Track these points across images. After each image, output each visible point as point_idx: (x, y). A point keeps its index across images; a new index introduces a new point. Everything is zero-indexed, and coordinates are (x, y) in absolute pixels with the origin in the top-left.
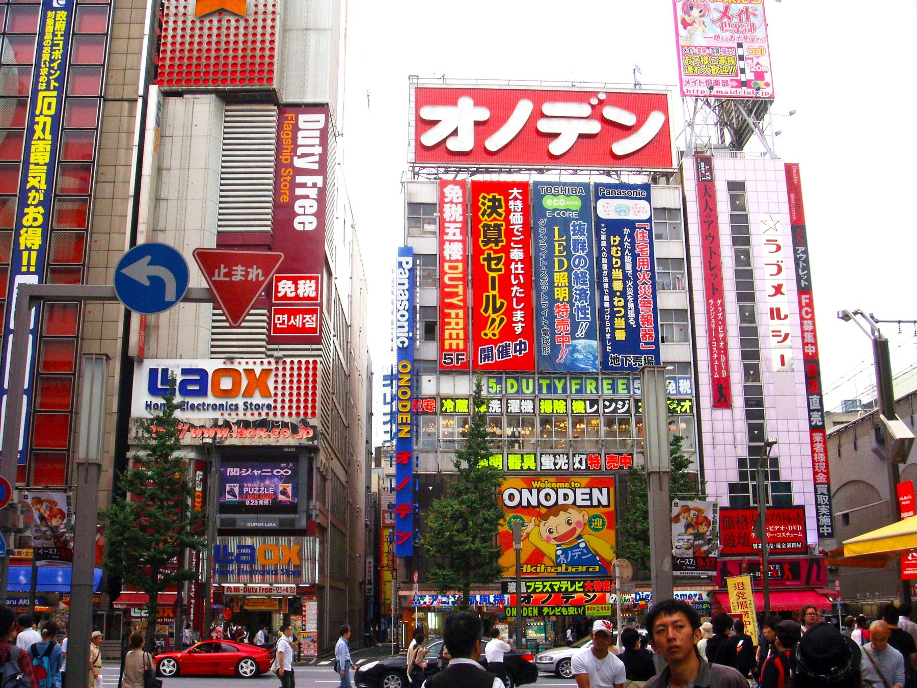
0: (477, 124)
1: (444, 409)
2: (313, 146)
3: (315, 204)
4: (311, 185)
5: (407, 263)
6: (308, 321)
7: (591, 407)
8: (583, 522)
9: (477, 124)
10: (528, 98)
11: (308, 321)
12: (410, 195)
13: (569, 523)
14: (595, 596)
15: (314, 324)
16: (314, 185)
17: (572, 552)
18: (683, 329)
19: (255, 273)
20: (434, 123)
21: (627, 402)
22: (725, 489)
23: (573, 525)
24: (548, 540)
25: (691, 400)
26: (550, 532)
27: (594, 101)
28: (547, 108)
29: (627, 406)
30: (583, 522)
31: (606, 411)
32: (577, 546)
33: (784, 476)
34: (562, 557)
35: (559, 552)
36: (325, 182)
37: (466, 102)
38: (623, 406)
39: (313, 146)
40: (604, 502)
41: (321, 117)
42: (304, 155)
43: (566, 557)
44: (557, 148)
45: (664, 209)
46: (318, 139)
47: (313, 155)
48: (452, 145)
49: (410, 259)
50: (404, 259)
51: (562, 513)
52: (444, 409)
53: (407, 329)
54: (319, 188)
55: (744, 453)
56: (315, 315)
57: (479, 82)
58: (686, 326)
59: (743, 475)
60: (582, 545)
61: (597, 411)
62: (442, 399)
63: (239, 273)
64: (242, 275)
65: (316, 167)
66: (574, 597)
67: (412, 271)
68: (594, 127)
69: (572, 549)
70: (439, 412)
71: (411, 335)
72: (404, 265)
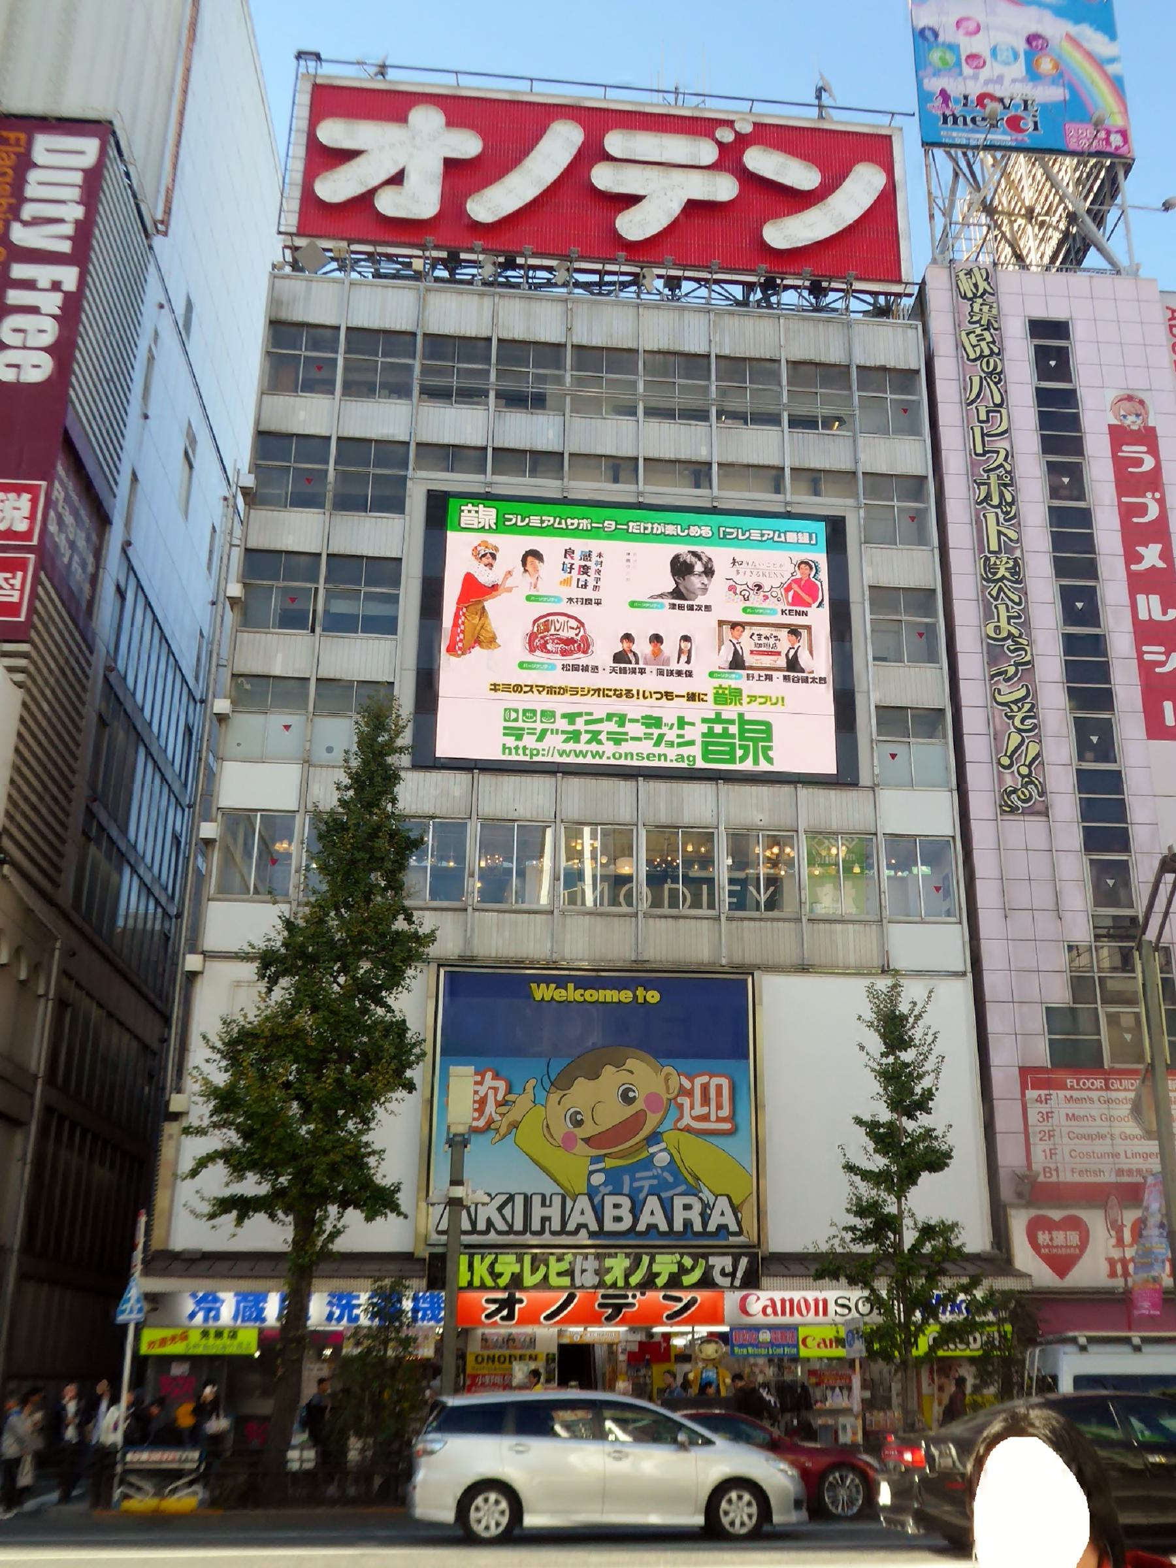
0: (452, 166)
4: (47, 285)
8: (665, 1096)
9: (452, 166)
10: (572, 118)
13: (626, 1098)
14: (693, 1301)
16: (56, 286)
17: (633, 1180)
18: (927, 633)
22: (1037, 1021)
23: (639, 1105)
24: (568, 1143)
27: (726, 136)
28: (615, 143)
30: (665, 1096)
32: (649, 1162)
36: (82, 282)
37: (426, 119)
41: (89, 147)
42: (37, 221)
47: (60, 221)
48: (388, 204)
51: (609, 1070)
54: (67, 295)
60: (662, 1159)
65: (65, 247)
66: (632, 1305)
68: (724, 188)
69: (631, 1170)
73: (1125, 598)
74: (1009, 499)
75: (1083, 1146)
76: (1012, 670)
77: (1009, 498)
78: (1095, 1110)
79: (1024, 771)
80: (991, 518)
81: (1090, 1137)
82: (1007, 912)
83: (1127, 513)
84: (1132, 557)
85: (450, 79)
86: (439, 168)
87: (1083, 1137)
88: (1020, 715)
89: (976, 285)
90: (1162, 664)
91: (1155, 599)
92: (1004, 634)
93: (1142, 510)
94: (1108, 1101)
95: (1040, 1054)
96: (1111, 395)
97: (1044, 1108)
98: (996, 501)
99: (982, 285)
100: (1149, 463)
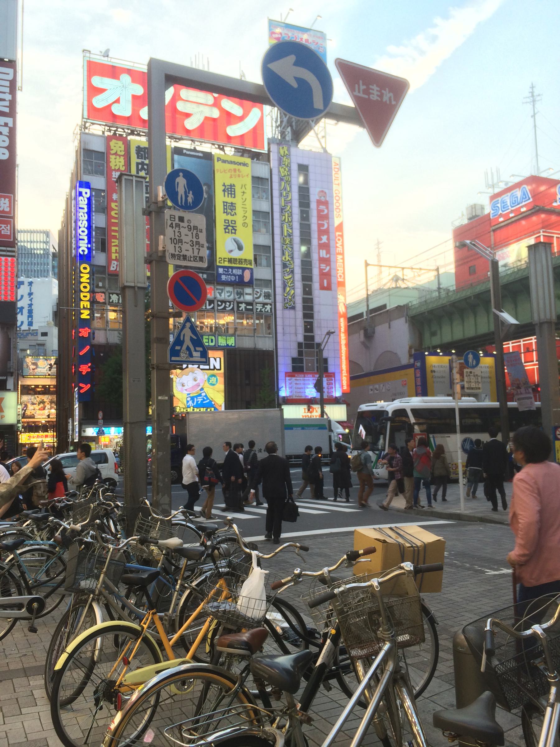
0: (134, 97)
1: (111, 301)
2: (4, 93)
3: (7, 140)
4: (3, 124)
5: (86, 193)
6: (3, 229)
7: (210, 305)
9: (134, 97)
11: (3, 229)
12: (85, 143)
13: (195, 380)
15: (9, 232)
16: (6, 125)
18: (268, 259)
19: (389, 95)
20: (102, 91)
21: (232, 303)
22: (289, 361)
25: (271, 305)
26: (183, 385)
29: (232, 306)
31: (219, 308)
33: (325, 354)
34: (190, 402)
35: (189, 399)
37: (126, 78)
38: (230, 306)
39: (4, 93)
40: (218, 367)
41: (10, 71)
43: (193, 402)
44: (191, 124)
45: (258, 178)
46: (8, 89)
47: (4, 100)
48: (116, 110)
49: (88, 191)
50: (84, 190)
51: (191, 374)
52: (111, 301)
53: (86, 241)
54: (10, 128)
55: (301, 339)
56: (9, 226)
57: (136, 65)
58: (270, 256)
59: (300, 353)
60: (203, 394)
61: (213, 308)
62: (110, 294)
63: (375, 93)
64: (378, 95)
65: (7, 110)
67: (89, 199)
68: (215, 113)
69: (197, 397)
70: (107, 302)
71: (89, 246)
72: (84, 194)
73: (317, 251)
74: (290, 220)
75: (298, 390)
76: (288, 270)
77: (290, 220)
78: (302, 382)
79: (290, 297)
80: (285, 226)
81: (300, 388)
82: (284, 334)
83: (320, 226)
84: (320, 239)
85: (132, 64)
86: (130, 98)
87: (298, 388)
88: (290, 283)
89: (284, 152)
90: (325, 269)
91: (324, 251)
92: (287, 260)
93: (323, 225)
94: (304, 380)
95: (290, 369)
96: (318, 190)
97: (290, 382)
98: (287, 221)
99: (286, 152)
100: (326, 212)
